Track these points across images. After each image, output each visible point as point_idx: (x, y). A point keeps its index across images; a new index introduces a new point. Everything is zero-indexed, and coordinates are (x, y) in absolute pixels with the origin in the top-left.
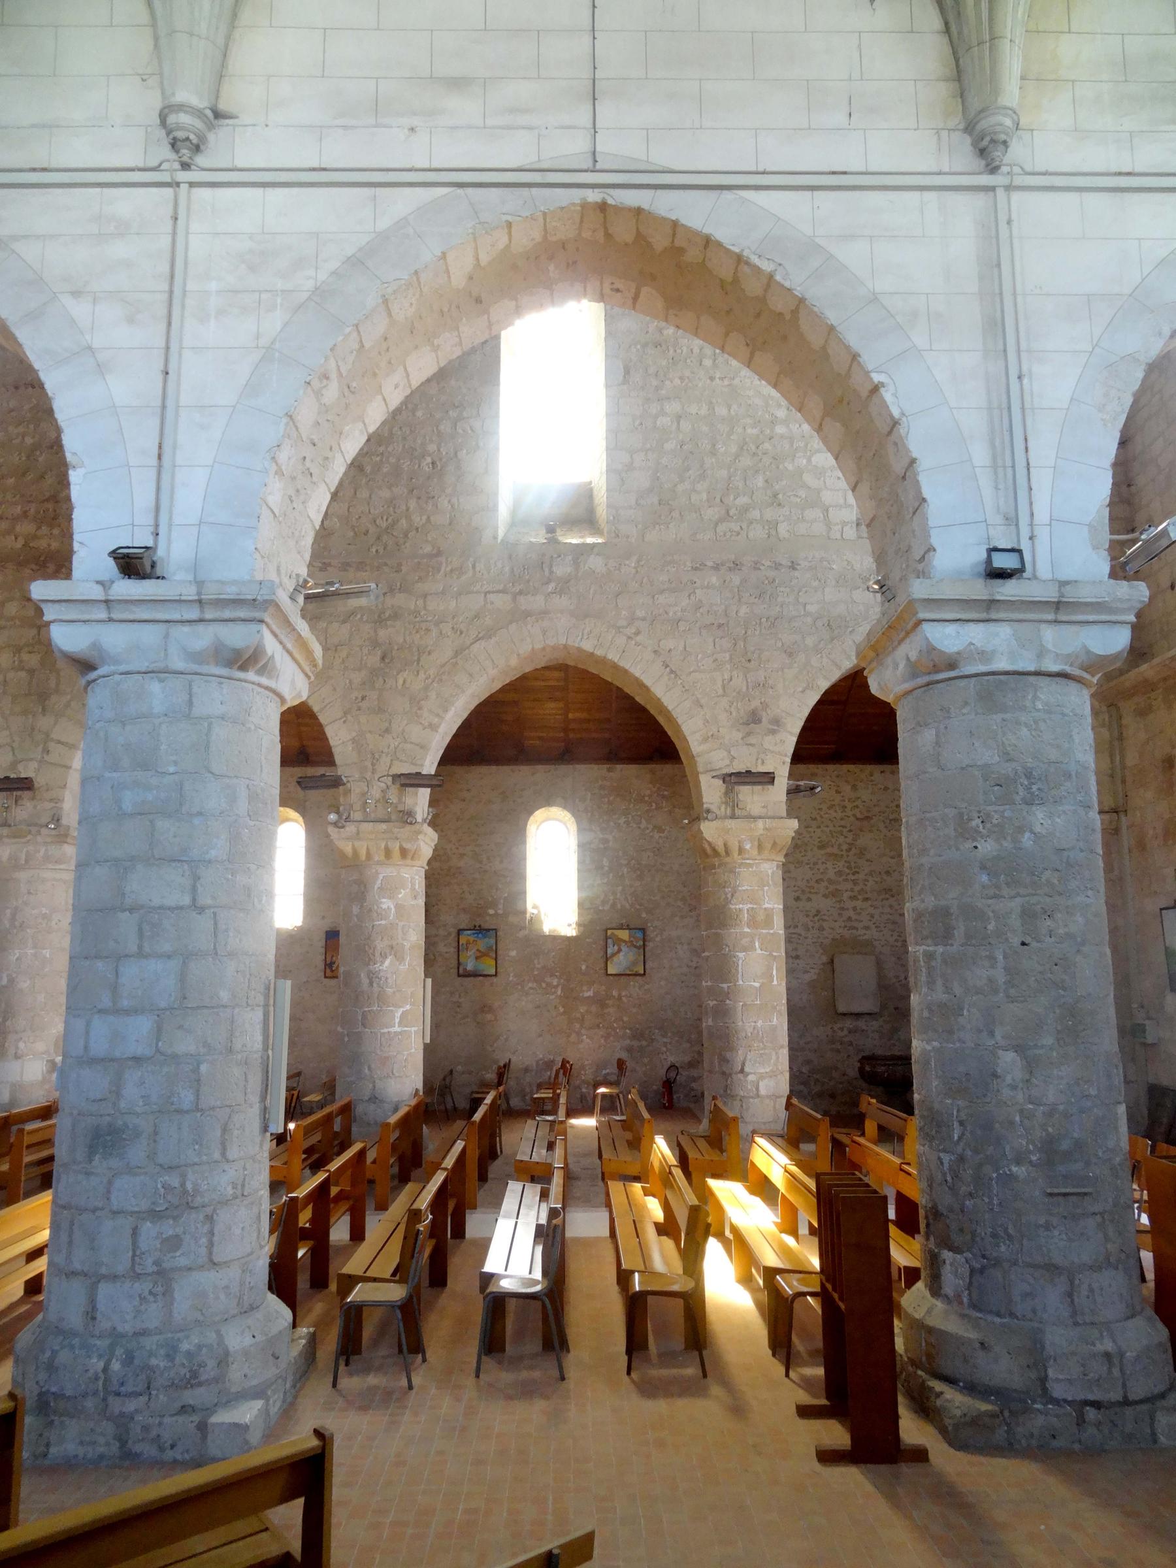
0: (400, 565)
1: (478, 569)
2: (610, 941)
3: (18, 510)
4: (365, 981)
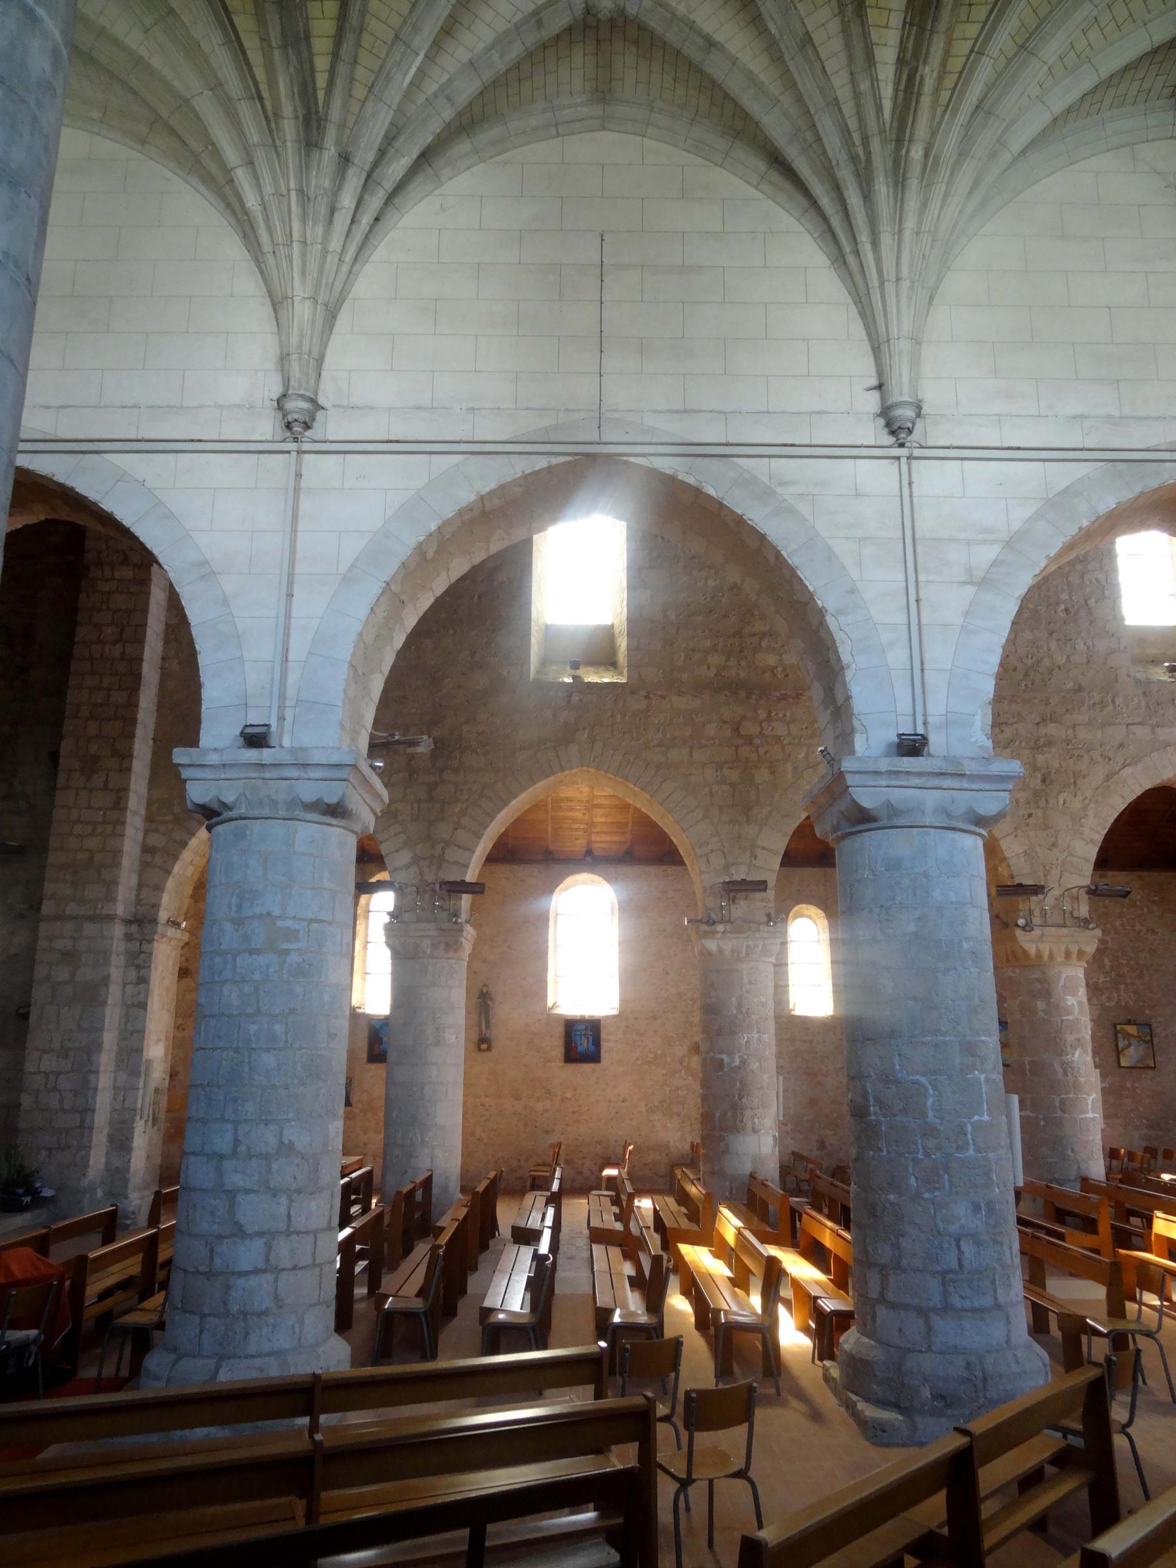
0: (1048, 698)
1: (1117, 703)
2: (1120, 1035)
3: (708, 643)
4: (1059, 1070)
